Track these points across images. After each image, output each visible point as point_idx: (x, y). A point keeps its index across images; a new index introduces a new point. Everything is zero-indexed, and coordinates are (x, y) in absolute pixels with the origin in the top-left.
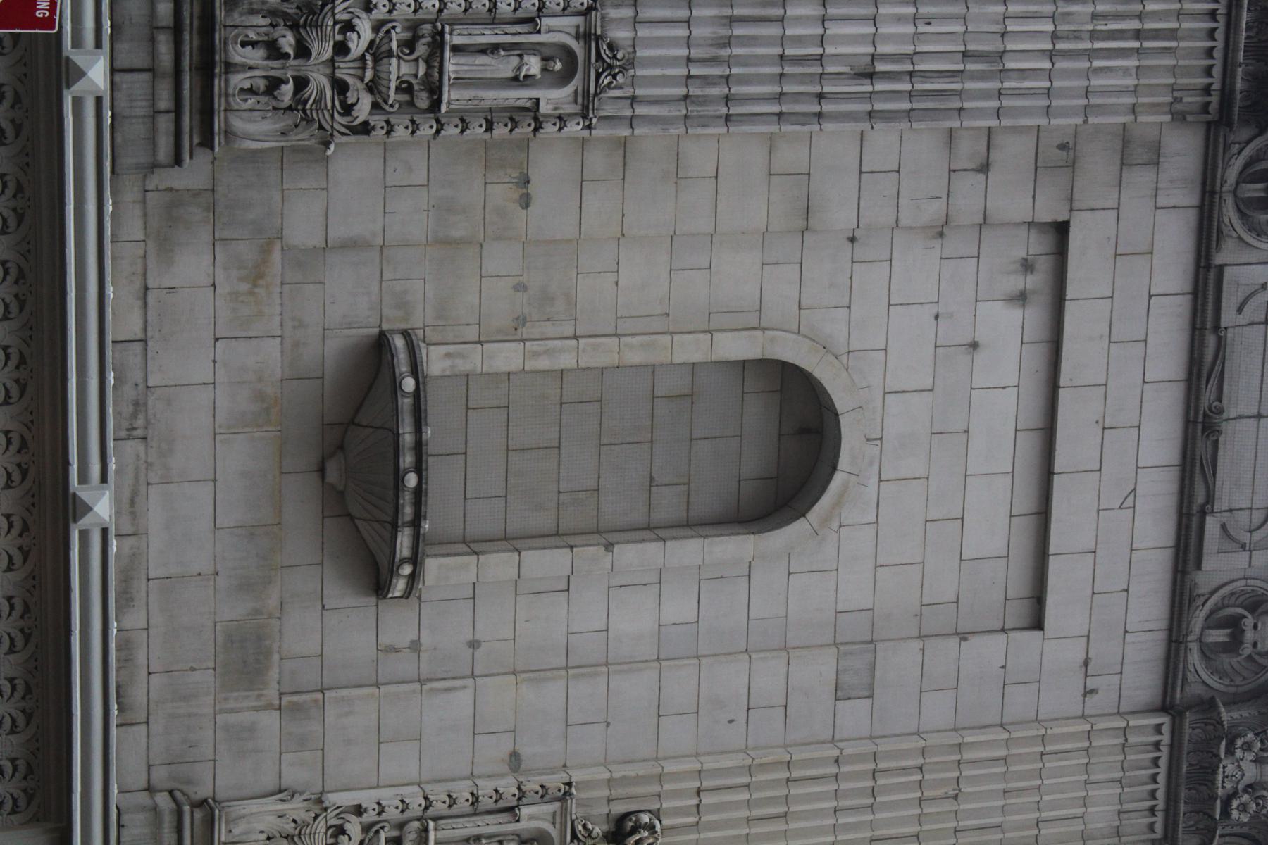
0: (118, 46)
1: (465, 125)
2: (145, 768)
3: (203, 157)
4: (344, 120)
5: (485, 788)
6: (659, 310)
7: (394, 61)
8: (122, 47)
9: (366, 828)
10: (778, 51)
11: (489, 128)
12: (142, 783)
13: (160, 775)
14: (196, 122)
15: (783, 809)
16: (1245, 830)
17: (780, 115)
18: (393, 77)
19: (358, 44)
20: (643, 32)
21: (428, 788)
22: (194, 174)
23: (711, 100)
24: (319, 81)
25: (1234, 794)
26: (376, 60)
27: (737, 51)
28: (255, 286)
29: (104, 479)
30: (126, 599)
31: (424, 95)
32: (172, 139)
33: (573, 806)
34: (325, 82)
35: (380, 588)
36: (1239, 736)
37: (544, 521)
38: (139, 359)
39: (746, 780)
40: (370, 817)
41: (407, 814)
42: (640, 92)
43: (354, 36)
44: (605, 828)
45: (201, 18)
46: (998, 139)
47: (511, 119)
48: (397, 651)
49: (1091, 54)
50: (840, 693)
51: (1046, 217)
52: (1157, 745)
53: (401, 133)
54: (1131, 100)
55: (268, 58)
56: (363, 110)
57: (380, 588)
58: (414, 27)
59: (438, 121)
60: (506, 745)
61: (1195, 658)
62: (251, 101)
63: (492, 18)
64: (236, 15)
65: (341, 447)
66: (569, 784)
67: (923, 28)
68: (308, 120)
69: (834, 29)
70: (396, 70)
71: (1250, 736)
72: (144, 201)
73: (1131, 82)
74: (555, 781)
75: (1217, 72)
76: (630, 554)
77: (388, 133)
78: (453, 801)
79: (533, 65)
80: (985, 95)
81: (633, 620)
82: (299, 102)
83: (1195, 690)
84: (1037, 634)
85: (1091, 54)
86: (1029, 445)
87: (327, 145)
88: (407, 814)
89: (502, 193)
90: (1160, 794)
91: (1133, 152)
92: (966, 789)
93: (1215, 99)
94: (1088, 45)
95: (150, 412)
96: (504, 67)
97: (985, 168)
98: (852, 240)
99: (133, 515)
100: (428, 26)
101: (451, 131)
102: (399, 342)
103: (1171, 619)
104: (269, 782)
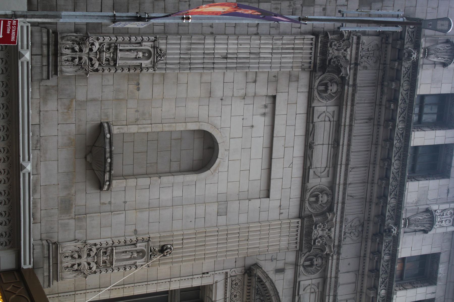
0: (33, 49)
1: (123, 70)
2: (40, 234)
3: (55, 77)
4: (92, 68)
5: (128, 239)
6: (173, 117)
7: (105, 53)
8: (34, 49)
9: (97, 249)
10: (203, 51)
11: (129, 71)
12: (39, 238)
13: (44, 236)
14: (53, 69)
15: (204, 244)
16: (319, 247)
17: (203, 68)
18: (104, 57)
19: (95, 49)
20: (169, 46)
21: (113, 239)
22: (52, 82)
23: (186, 64)
24: (85, 58)
25: (317, 239)
26: (100, 53)
27: (192, 51)
28: (68, 110)
29: (29, 160)
30: (35, 191)
31: (112, 62)
32: (47, 73)
33: (150, 243)
34: (87, 58)
35: (100, 187)
36: (318, 224)
37: (143, 171)
38: (38, 129)
39: (194, 236)
40: (98, 246)
41: (108, 246)
42: (167, 62)
43: (94, 47)
44: (159, 249)
45: (55, 42)
46: (258, 75)
47: (135, 68)
48: (105, 204)
49: (282, 53)
50: (219, 214)
51: (270, 94)
52: (298, 227)
53: (106, 71)
54: (291, 65)
55: (72, 52)
56: (96, 66)
57: (100, 187)
58: (110, 44)
59: (116, 68)
60: (133, 228)
61: (307, 205)
62: (67, 63)
63: (130, 43)
64: (63, 41)
65: (91, 152)
66: (150, 238)
67: (239, 46)
68: (82, 68)
69: (217, 46)
70: (105, 55)
71: (320, 224)
72: (39, 89)
73: (291, 60)
74: (146, 237)
75: (313, 58)
76: (166, 179)
77: (103, 71)
78: (120, 242)
79: (140, 54)
80: (255, 63)
81: (166, 196)
82: (80, 63)
83: (307, 213)
84: (268, 199)
85: (282, 53)
86: (266, 151)
87: (87, 74)
88: (108, 246)
89: (132, 87)
90: (298, 239)
91: (292, 78)
92: (250, 238)
93: (312, 65)
94: (281, 51)
95: (41, 143)
96: (133, 55)
97: (255, 82)
98: (222, 99)
99: (37, 169)
100: (113, 44)
101: (119, 71)
102: (106, 125)
103: (301, 195)
104: (72, 237)
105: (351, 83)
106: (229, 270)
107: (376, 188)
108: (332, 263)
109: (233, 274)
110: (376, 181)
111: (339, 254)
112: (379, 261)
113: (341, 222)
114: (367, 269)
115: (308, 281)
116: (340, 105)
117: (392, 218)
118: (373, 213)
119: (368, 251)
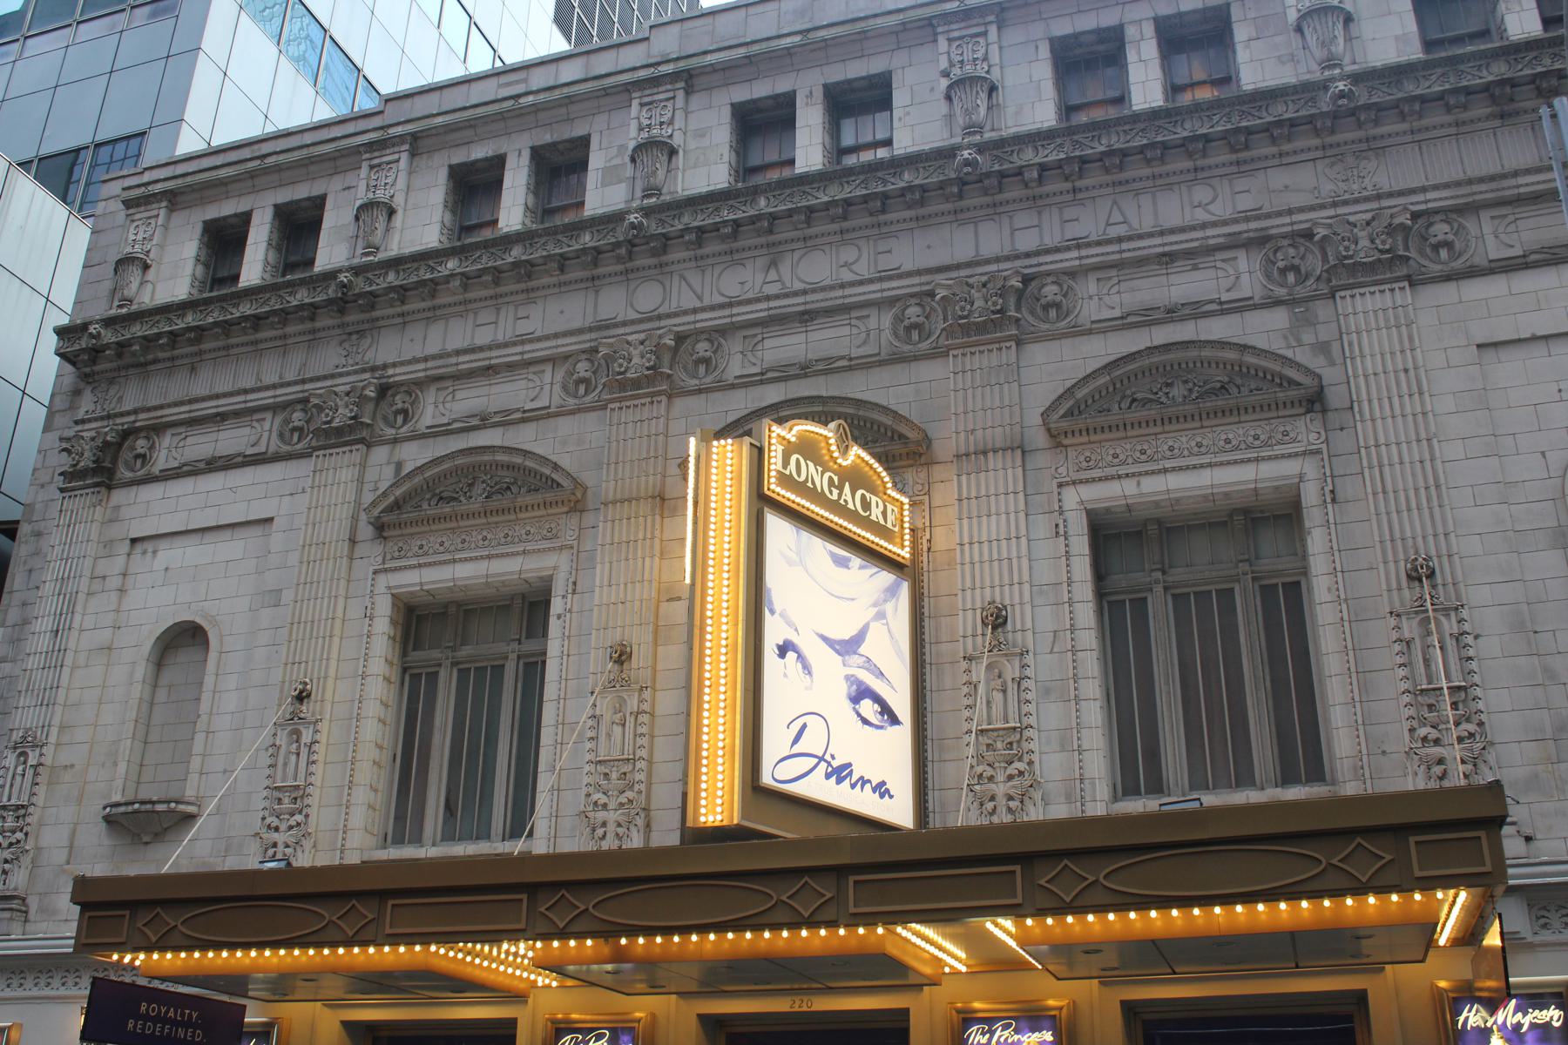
57: (191, 818)
86: (208, 537)
89: (67, 777)
97: (104, 577)
105: (132, 418)
106: (371, 569)
107: (290, 329)
108: (398, 375)
109: (380, 559)
110: (280, 332)
111: (385, 367)
112: (404, 288)
113: (333, 376)
114: (423, 305)
115: (429, 412)
116: (158, 429)
117: (327, 287)
118: (329, 322)
119: (390, 311)
